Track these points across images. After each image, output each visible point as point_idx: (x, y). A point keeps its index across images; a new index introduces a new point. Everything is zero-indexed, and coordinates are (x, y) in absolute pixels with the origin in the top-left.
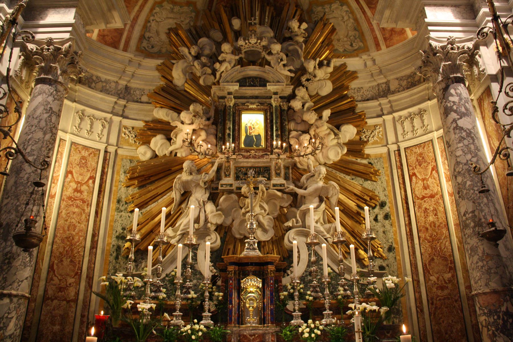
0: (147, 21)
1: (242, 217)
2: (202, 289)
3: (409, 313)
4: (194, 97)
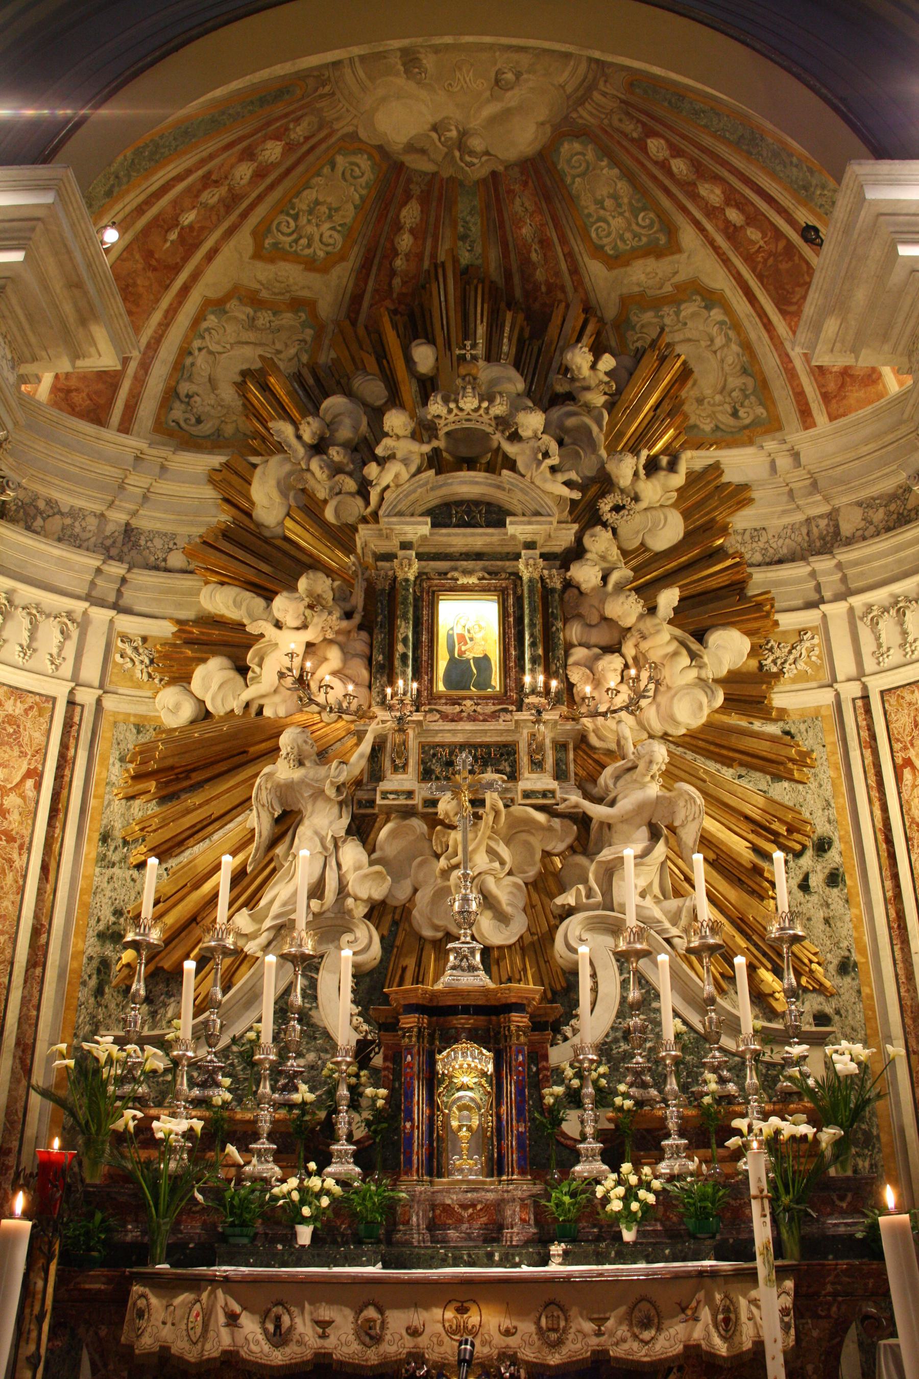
0: (185, 351)
1: (439, 881)
2: (330, 1077)
3: (898, 1144)
4: (311, 556)
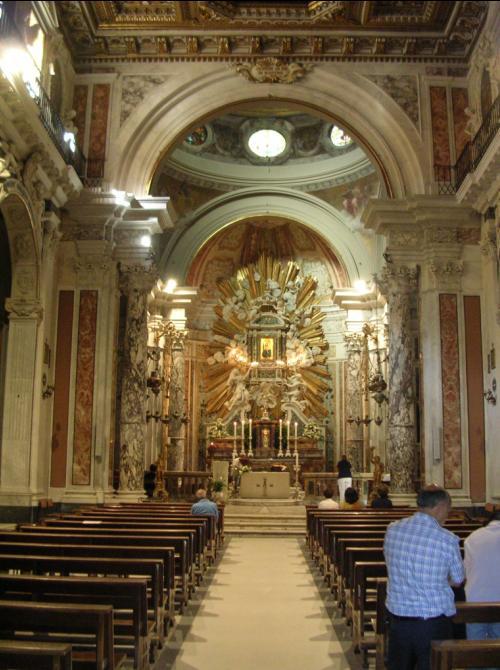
0: (205, 274)
